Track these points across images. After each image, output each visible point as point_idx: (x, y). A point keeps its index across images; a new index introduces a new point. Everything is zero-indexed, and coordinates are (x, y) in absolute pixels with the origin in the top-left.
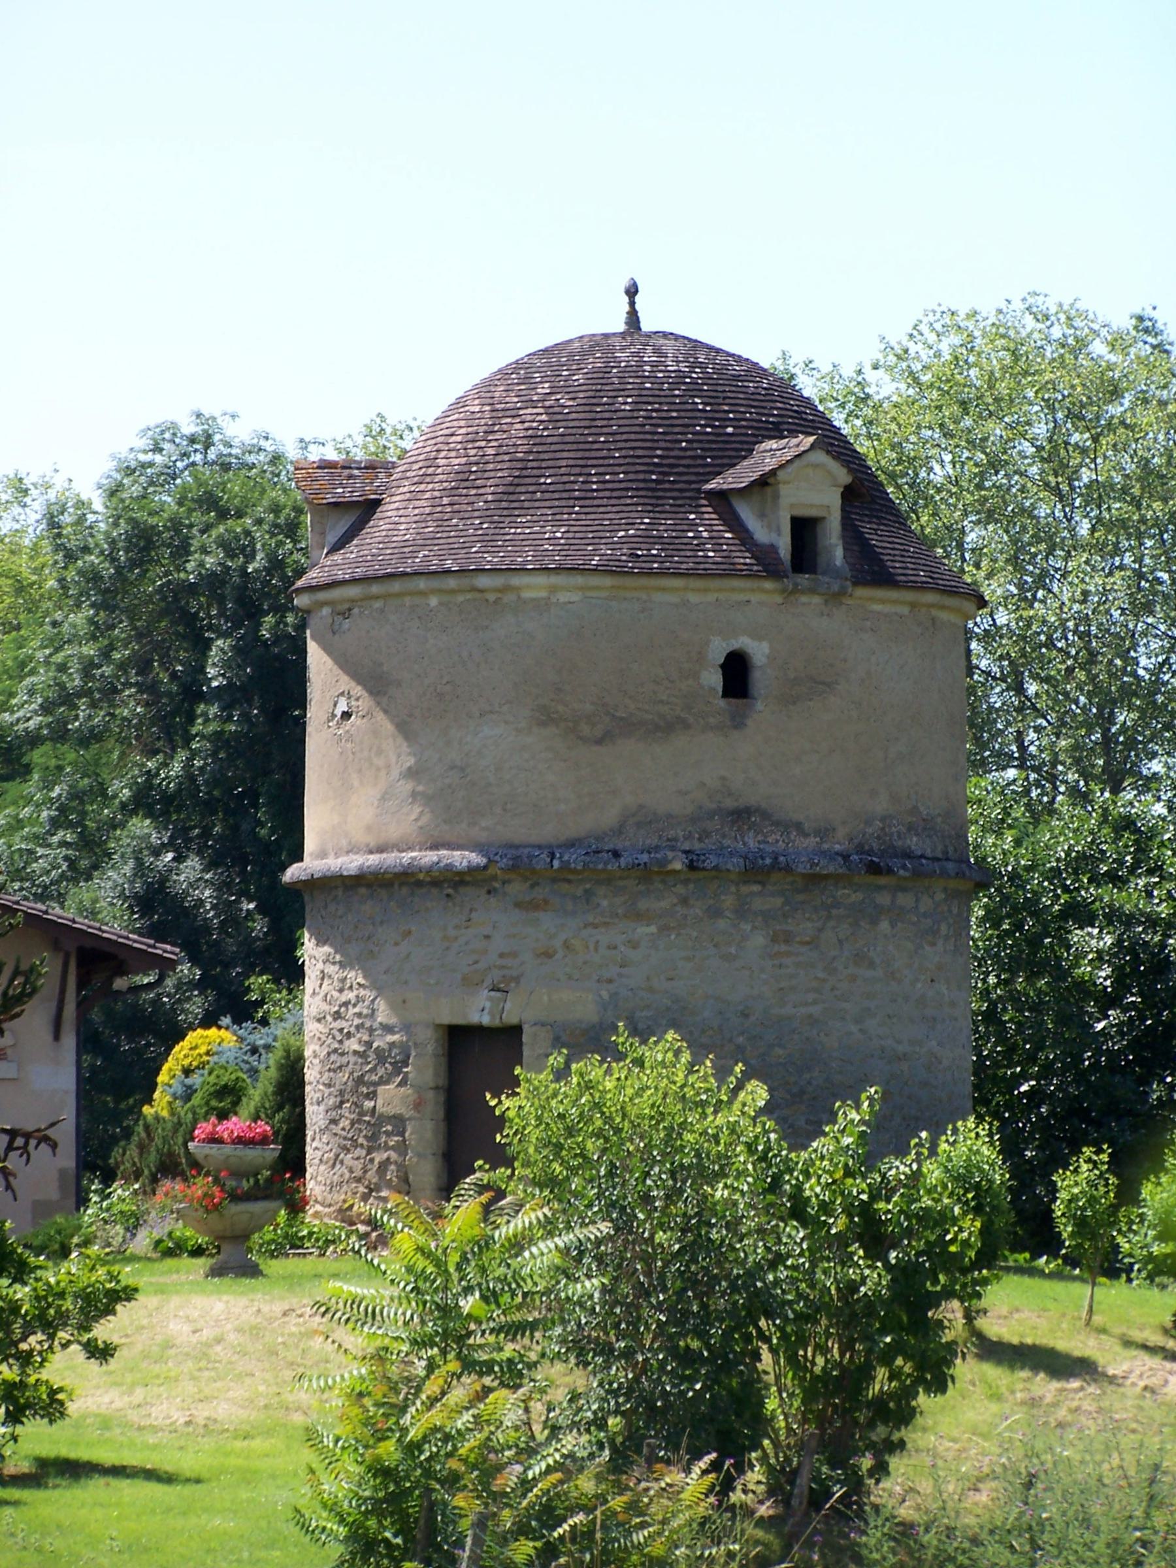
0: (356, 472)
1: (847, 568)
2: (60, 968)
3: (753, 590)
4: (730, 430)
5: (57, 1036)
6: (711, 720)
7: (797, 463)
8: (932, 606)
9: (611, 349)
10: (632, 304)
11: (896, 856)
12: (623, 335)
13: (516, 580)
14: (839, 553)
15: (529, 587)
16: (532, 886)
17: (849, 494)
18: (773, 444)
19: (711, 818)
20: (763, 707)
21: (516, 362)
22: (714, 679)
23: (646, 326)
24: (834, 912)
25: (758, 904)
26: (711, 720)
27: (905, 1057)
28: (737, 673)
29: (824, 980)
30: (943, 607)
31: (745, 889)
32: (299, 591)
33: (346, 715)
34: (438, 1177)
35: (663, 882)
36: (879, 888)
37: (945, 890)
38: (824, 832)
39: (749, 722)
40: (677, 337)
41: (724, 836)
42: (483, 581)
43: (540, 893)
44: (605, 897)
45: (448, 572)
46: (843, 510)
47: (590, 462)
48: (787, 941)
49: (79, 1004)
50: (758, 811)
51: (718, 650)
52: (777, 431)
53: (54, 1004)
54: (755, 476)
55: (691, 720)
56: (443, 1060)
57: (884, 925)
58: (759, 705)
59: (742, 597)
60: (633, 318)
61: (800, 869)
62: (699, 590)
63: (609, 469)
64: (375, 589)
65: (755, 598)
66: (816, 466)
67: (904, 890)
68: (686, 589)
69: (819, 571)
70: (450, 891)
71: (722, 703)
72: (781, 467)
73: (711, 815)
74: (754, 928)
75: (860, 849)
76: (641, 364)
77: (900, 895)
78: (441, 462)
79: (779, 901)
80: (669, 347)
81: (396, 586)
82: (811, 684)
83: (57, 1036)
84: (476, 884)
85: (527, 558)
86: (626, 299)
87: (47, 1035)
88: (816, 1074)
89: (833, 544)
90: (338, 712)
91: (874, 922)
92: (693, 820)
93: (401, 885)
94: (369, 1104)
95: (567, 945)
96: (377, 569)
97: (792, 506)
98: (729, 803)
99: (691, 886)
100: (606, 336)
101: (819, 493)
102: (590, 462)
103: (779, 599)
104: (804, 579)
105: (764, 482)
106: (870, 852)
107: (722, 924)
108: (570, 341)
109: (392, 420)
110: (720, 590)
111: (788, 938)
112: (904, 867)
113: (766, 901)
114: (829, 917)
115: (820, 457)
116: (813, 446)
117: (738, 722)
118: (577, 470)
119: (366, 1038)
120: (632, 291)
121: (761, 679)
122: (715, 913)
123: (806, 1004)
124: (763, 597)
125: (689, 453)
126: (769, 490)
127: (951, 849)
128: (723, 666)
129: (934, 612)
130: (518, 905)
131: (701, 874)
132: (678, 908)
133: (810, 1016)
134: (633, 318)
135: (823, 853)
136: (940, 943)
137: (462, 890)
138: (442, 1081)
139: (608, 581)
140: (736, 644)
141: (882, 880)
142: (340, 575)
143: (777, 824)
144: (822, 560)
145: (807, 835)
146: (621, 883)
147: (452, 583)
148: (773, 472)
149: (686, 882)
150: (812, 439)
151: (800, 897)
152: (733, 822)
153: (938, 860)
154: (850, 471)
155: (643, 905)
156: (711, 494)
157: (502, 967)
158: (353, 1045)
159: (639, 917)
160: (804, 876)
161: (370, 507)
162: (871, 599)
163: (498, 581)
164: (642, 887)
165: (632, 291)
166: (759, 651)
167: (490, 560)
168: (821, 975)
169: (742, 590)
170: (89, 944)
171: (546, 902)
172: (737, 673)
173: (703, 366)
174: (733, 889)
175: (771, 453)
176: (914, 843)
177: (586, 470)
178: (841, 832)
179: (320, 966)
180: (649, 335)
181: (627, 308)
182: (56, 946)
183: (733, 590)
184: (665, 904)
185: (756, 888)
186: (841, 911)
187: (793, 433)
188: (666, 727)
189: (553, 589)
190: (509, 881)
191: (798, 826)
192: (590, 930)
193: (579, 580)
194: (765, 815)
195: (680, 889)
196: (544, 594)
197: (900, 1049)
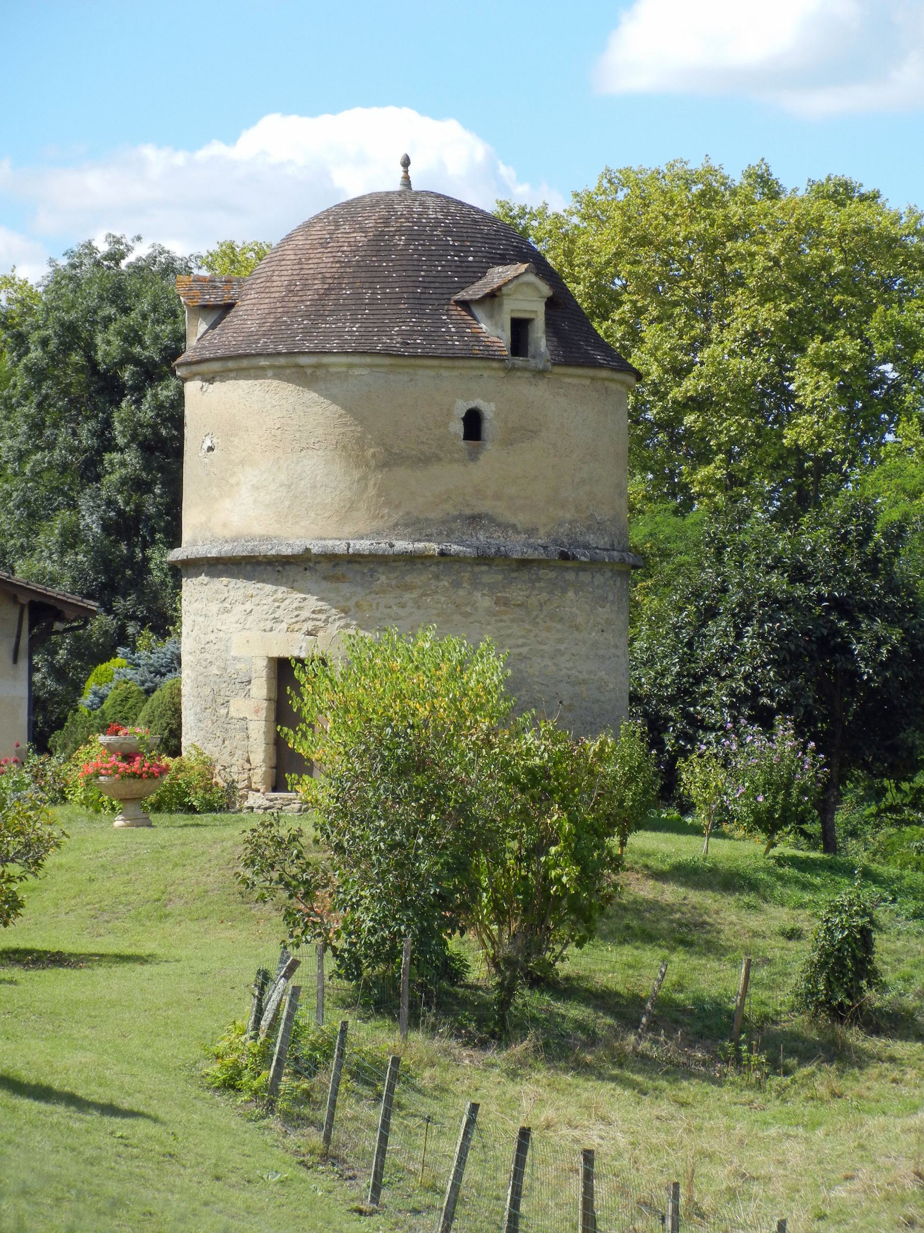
0: (218, 284)
1: (548, 353)
2: (17, 616)
3: (485, 368)
4: (471, 259)
5: (15, 660)
6: (456, 455)
7: (515, 282)
8: (606, 379)
9: (390, 206)
10: (406, 172)
11: (579, 547)
12: (400, 193)
13: (326, 360)
14: (543, 343)
15: (334, 365)
16: (335, 566)
17: (551, 303)
18: (500, 269)
19: (455, 521)
20: (491, 448)
21: (327, 211)
22: (458, 428)
23: (415, 187)
24: (537, 584)
25: (486, 579)
26: (456, 455)
27: (584, 682)
28: (473, 424)
29: (530, 631)
30: (613, 380)
31: (477, 569)
32: (179, 365)
33: (211, 449)
34: (269, 689)
35: (422, 564)
36: (567, 569)
37: (612, 571)
38: (531, 531)
39: (481, 457)
40: (438, 196)
41: (464, 534)
42: (303, 360)
43: (339, 571)
44: (383, 573)
45: (279, 354)
46: (546, 314)
47: (376, 280)
48: (505, 604)
49: (30, 640)
50: (487, 515)
51: (461, 408)
52: (503, 260)
53: (14, 640)
54: (488, 291)
55: (442, 455)
56: (275, 682)
57: (571, 594)
58: (489, 446)
59: (479, 373)
60: (407, 181)
61: (515, 556)
62: (447, 368)
63: (389, 285)
64: (231, 364)
65: (486, 373)
66: (528, 284)
67: (584, 570)
68: (440, 367)
69: (530, 354)
70: (280, 568)
71: (462, 443)
72: (505, 284)
73: (455, 519)
74: (483, 595)
75: (555, 542)
76: (411, 212)
77: (581, 573)
78: (275, 278)
79: (500, 577)
80: (430, 202)
81: (245, 363)
82: (522, 433)
83: (15, 660)
84: (297, 564)
85: (334, 345)
86: (402, 168)
87: (9, 661)
88: (524, 692)
89: (539, 336)
90: (205, 447)
91: (564, 591)
92: (443, 522)
93: (247, 563)
94: (223, 711)
95: (357, 605)
96: (232, 351)
97: (512, 311)
98: (468, 512)
99: (441, 567)
100: (388, 193)
101: (530, 302)
102: (376, 280)
103: (502, 374)
104: (519, 361)
105: (493, 296)
106: (562, 544)
107: (461, 593)
108: (364, 197)
109: (239, 243)
110: (463, 368)
111: (506, 602)
112: (584, 555)
113: (490, 577)
114: (534, 588)
115: (532, 278)
116: (526, 271)
117: (473, 456)
118: (367, 285)
119: (223, 665)
120: (406, 163)
121: (489, 427)
122: (457, 585)
123: (518, 646)
124: (493, 373)
125: (442, 274)
126: (497, 300)
127: (616, 544)
128: (464, 419)
129: (607, 383)
130: (325, 578)
131: (448, 559)
132: (432, 581)
133: (520, 654)
134: (407, 181)
135: (530, 546)
136: (608, 605)
137: (287, 567)
138: (274, 696)
139: (387, 361)
140: (472, 404)
141: (570, 564)
142: (207, 355)
143: (499, 525)
144: (531, 349)
145: (519, 533)
146: (394, 564)
147: (282, 361)
148: (499, 288)
149: (438, 564)
150: (526, 265)
151: (514, 575)
152: (470, 524)
153: (607, 550)
154: (552, 286)
155: (408, 579)
156: (458, 303)
157: (313, 619)
158: (214, 670)
159: (409, 588)
160: (516, 560)
161: (227, 308)
162: (565, 375)
163: (313, 360)
164: (408, 568)
165: (406, 163)
166: (488, 409)
167: (308, 346)
168: (527, 627)
169: (479, 368)
170: (37, 599)
171: (344, 576)
172: (473, 424)
173: (453, 215)
174: (469, 569)
175: (498, 275)
176: (591, 539)
177: (373, 285)
178: (542, 532)
179: (192, 617)
180: (417, 193)
181: (402, 174)
182: (14, 599)
183: (472, 368)
184: (424, 578)
185: (484, 568)
186: (542, 584)
187: (512, 261)
188: (424, 460)
189: (351, 366)
190: (319, 562)
191: (514, 527)
192: (373, 595)
193: (368, 360)
194: (492, 520)
195: (434, 568)
196: (344, 369)
197: (581, 677)
